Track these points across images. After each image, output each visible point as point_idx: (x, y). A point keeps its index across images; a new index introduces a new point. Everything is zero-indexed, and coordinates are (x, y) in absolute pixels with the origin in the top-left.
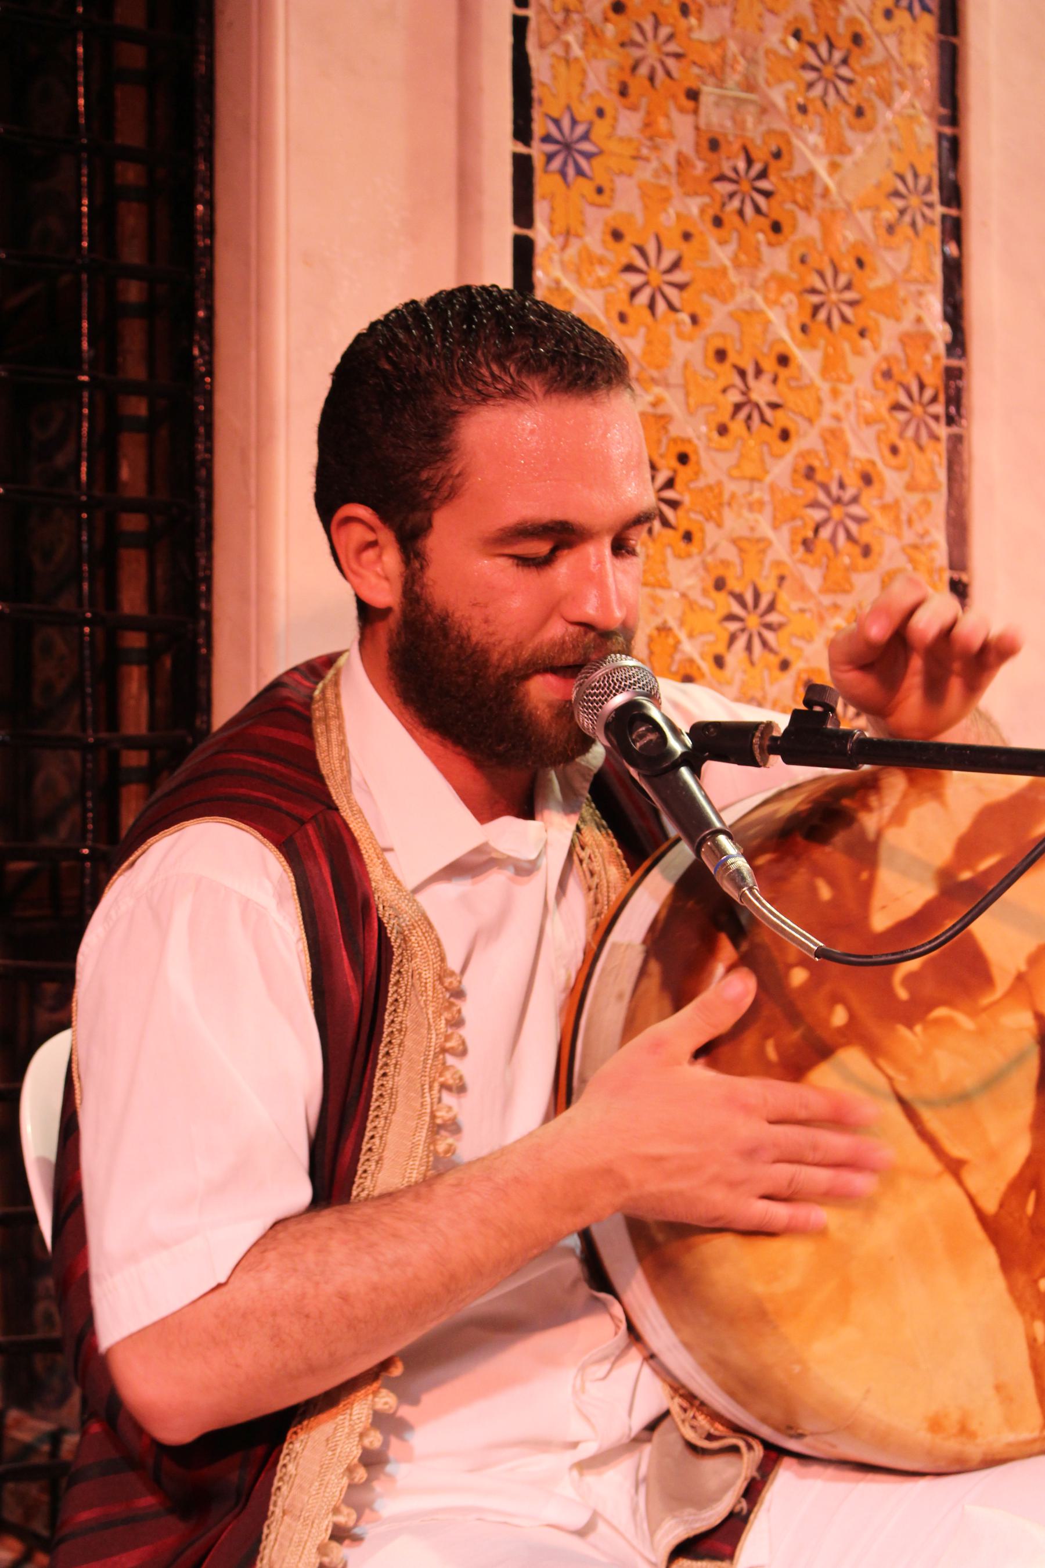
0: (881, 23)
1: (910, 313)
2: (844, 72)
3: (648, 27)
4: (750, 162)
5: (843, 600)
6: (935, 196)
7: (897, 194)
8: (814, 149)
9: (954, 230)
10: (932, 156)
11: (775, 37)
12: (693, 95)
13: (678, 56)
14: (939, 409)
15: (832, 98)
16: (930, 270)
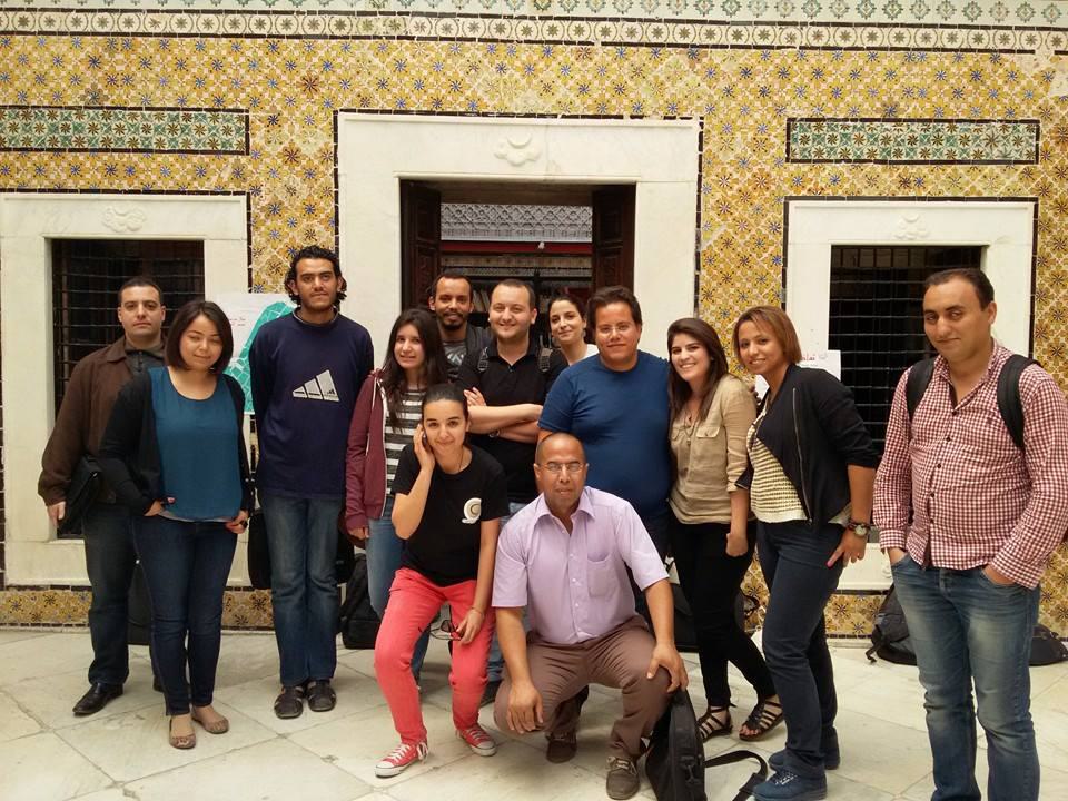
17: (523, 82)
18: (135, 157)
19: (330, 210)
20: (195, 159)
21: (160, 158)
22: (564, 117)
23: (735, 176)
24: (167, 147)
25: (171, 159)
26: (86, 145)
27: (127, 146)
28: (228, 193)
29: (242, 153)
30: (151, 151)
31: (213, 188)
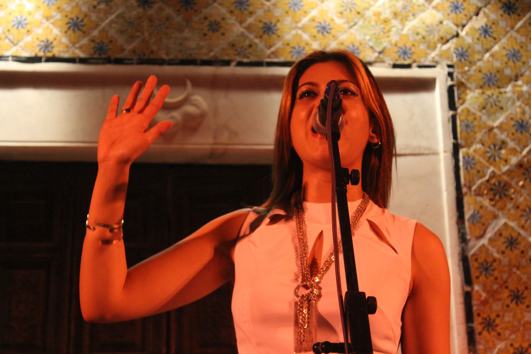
17: (178, 19)
22: (240, 64)
23: (511, 144)
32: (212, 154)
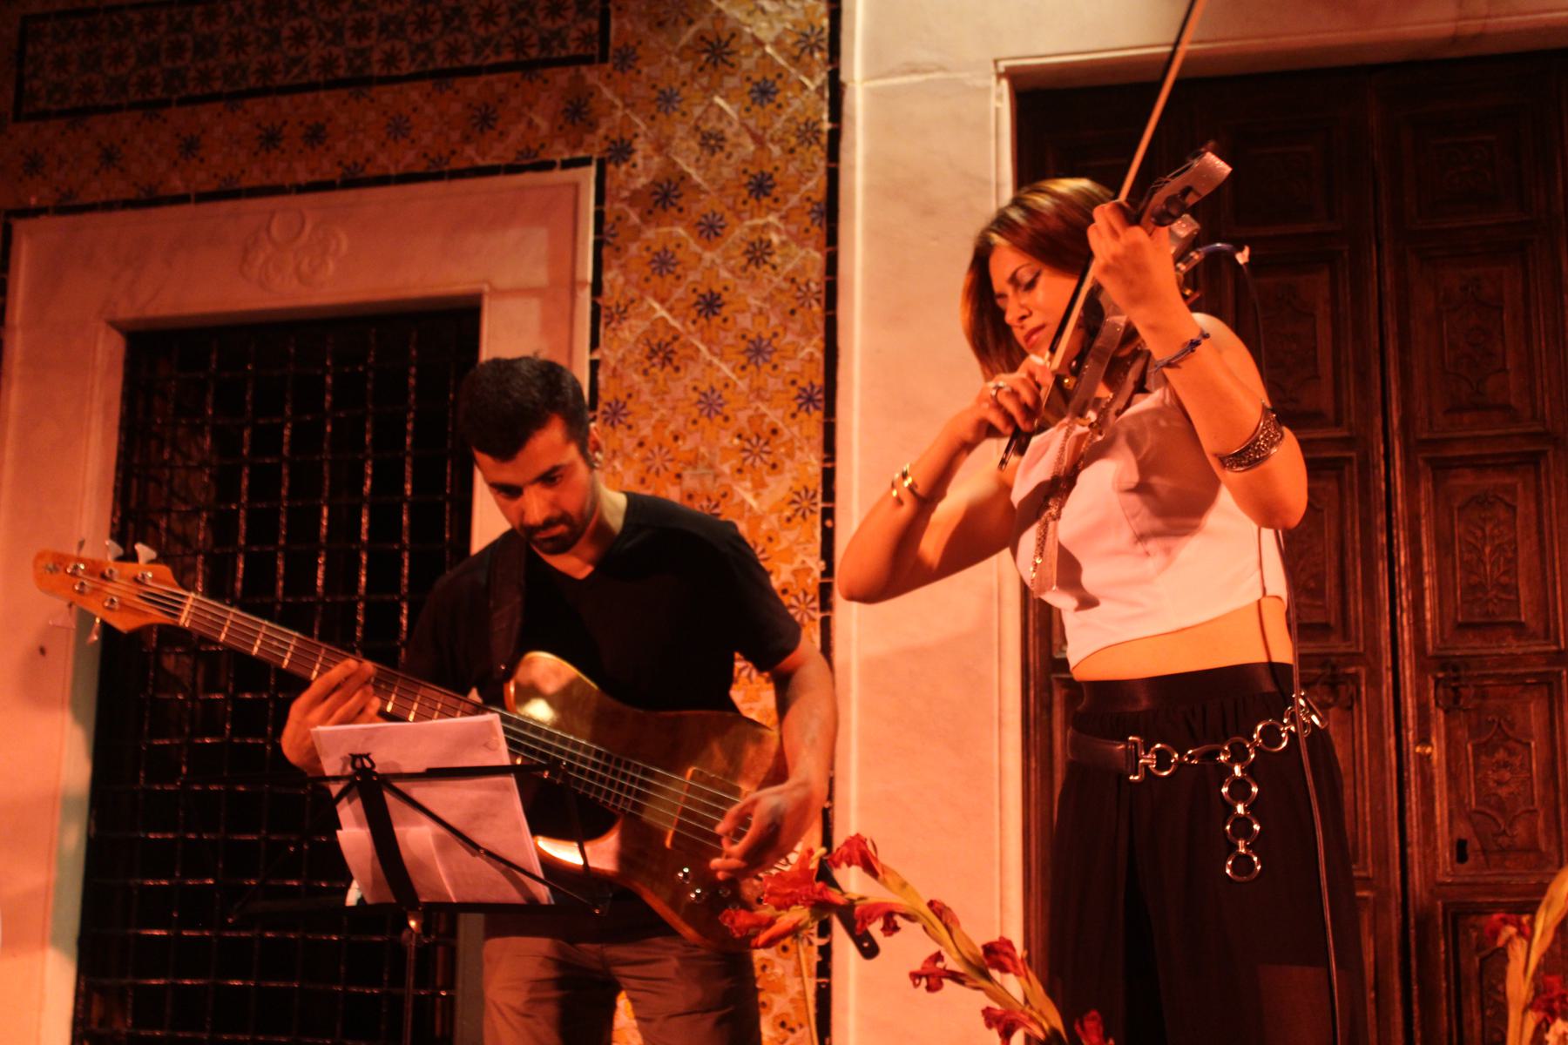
0: (789, 420)
1: (800, 557)
2: (767, 448)
3: (656, 449)
4: (709, 500)
5: (754, 705)
6: (819, 497)
7: (794, 502)
8: (746, 489)
9: (828, 514)
10: (819, 479)
11: (729, 440)
12: (679, 476)
13: (671, 460)
14: (816, 604)
15: (758, 463)
16: (813, 536)
18: (328, 101)
19: (815, 184)
20: (472, 88)
21: (386, 95)
24: (406, 67)
25: (414, 95)
26: (217, 86)
27: (313, 75)
28: (548, 166)
29: (588, 60)
30: (369, 81)
31: (511, 157)
32: (1455, 40)
